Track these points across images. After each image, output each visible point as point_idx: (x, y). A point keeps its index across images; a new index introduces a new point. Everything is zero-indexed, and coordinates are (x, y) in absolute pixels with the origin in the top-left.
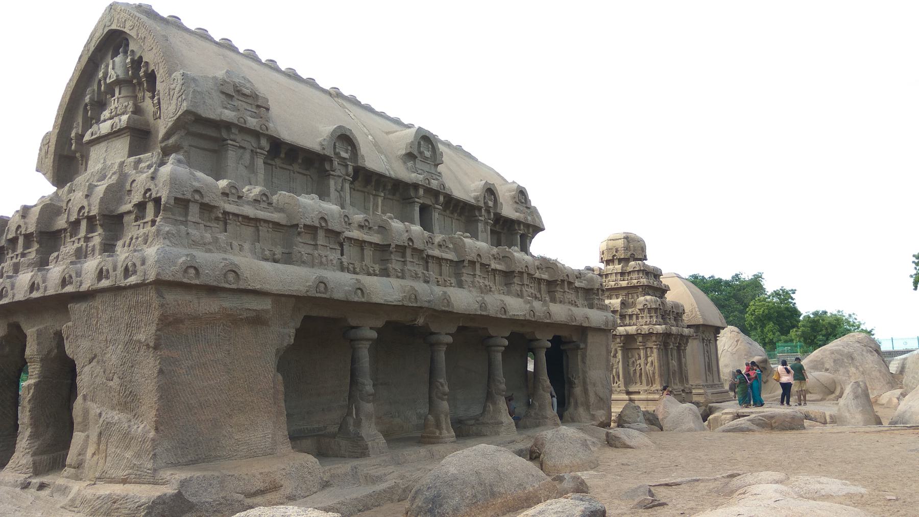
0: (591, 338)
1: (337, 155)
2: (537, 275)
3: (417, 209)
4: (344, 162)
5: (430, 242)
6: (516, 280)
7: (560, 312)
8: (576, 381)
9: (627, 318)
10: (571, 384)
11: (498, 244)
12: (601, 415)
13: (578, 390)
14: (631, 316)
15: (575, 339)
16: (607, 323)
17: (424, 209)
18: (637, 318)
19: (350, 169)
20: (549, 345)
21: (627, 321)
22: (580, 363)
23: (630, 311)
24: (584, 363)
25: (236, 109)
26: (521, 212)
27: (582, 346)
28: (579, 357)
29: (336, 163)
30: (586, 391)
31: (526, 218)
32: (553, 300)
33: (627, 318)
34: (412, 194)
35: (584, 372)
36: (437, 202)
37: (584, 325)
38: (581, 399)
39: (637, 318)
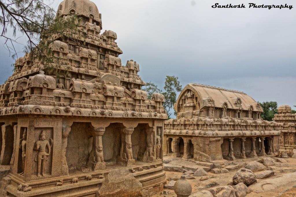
0: (274, 137)
1: (224, 107)
2: (262, 125)
3: (237, 114)
4: (225, 108)
5: (241, 122)
6: (258, 127)
7: (267, 132)
8: (271, 146)
9: (285, 128)
10: (269, 147)
11: (254, 119)
12: (276, 154)
13: (271, 148)
14: (286, 128)
15: (270, 137)
16: (278, 133)
17: (239, 113)
18: (288, 128)
19: (226, 109)
20: (265, 139)
21: (285, 129)
22: (272, 142)
23: (286, 126)
24: (272, 142)
25: (211, 104)
26: (258, 109)
27: (272, 139)
28: (271, 141)
29: (224, 109)
30: (273, 148)
31: (259, 110)
32: (266, 130)
33: (285, 128)
34: (236, 111)
35: (273, 144)
36: (241, 111)
37: (273, 135)
38: (271, 150)
39: (288, 128)
